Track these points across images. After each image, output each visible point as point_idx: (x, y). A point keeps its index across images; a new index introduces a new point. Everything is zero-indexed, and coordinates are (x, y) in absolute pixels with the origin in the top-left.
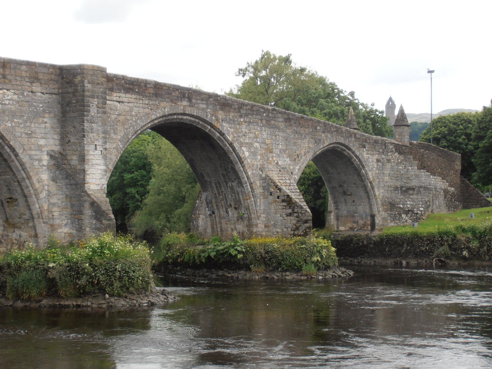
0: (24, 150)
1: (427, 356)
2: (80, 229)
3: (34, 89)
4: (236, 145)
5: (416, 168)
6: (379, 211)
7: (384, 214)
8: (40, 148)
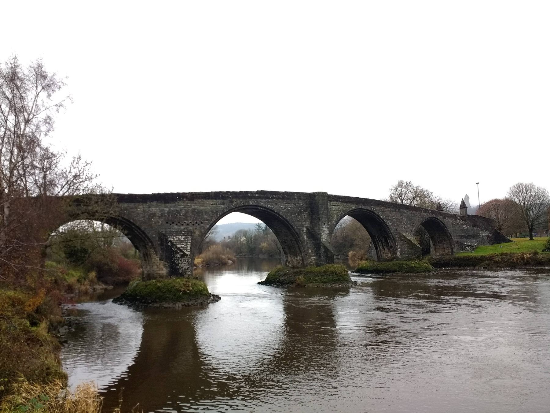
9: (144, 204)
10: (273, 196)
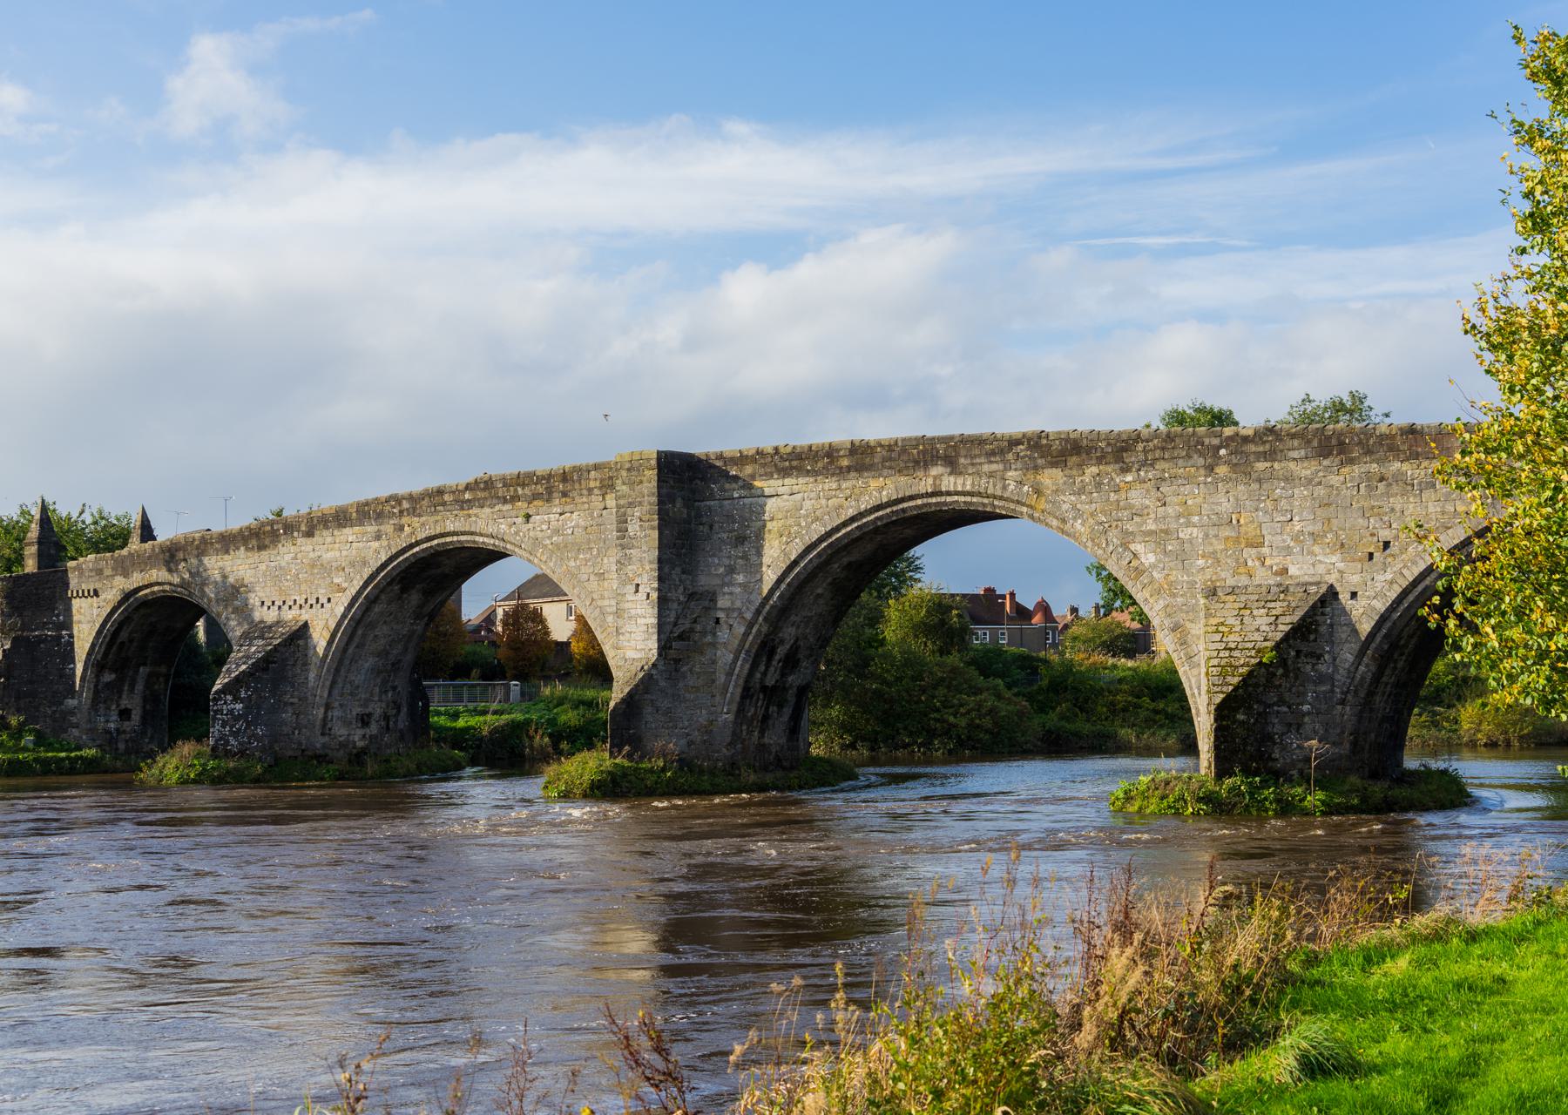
0: (593, 600)
1: (204, 902)
10: (516, 490)
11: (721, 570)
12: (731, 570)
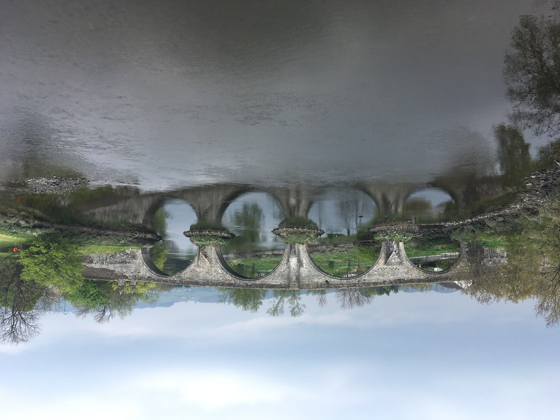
2: (298, 248)
3: (308, 283)
4: (225, 273)
5: (116, 271)
6: (140, 254)
7: (137, 253)
8: (306, 268)
9: (412, 278)
11: (286, 271)
12: (284, 271)
